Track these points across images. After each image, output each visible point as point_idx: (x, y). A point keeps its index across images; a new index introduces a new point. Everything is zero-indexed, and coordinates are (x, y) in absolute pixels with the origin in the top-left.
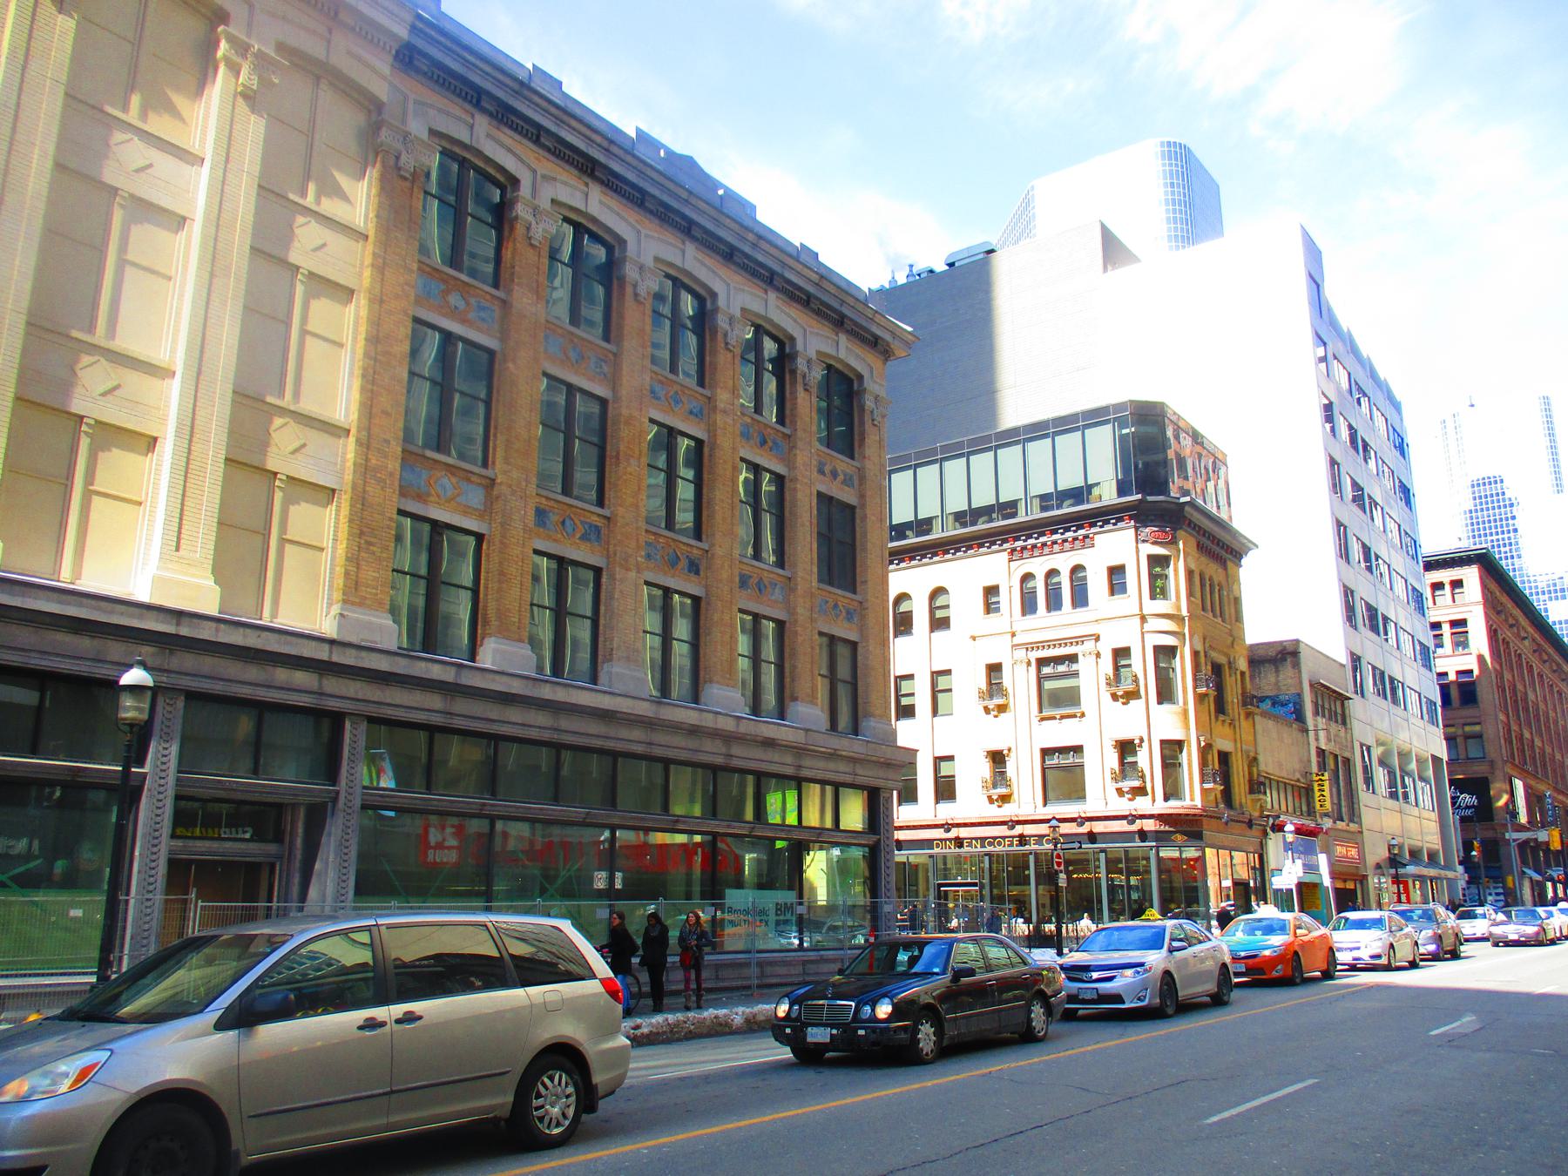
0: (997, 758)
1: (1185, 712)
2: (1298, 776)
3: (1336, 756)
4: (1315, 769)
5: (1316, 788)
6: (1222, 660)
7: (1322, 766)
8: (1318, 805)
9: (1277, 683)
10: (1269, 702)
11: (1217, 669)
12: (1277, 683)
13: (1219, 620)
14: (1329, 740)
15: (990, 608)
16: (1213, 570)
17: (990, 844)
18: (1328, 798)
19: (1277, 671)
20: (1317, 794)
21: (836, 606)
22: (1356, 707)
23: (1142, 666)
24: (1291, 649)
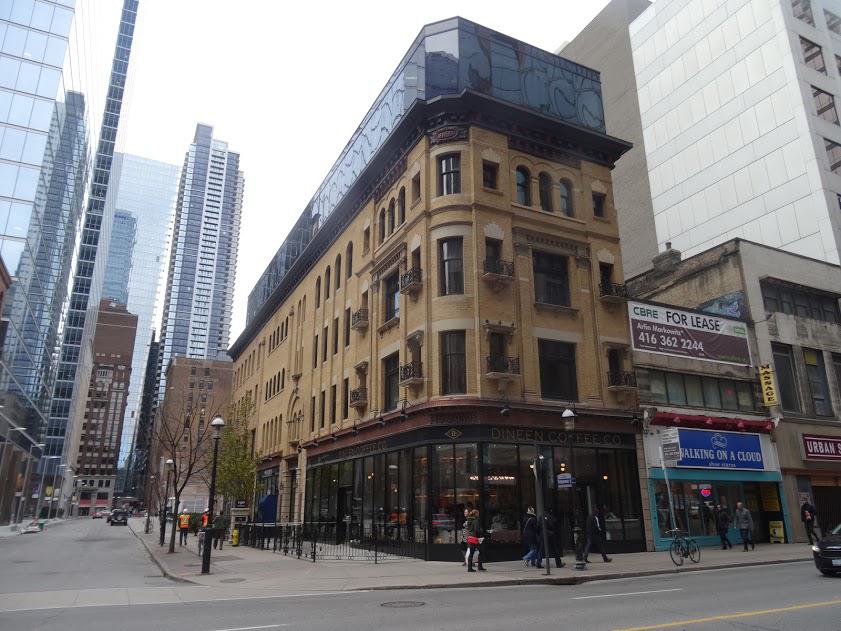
1: (469, 303)
3: (819, 353)
5: (763, 381)
8: (766, 398)
9: (722, 283)
12: (722, 283)
19: (721, 274)
20: (764, 387)
24: (730, 248)
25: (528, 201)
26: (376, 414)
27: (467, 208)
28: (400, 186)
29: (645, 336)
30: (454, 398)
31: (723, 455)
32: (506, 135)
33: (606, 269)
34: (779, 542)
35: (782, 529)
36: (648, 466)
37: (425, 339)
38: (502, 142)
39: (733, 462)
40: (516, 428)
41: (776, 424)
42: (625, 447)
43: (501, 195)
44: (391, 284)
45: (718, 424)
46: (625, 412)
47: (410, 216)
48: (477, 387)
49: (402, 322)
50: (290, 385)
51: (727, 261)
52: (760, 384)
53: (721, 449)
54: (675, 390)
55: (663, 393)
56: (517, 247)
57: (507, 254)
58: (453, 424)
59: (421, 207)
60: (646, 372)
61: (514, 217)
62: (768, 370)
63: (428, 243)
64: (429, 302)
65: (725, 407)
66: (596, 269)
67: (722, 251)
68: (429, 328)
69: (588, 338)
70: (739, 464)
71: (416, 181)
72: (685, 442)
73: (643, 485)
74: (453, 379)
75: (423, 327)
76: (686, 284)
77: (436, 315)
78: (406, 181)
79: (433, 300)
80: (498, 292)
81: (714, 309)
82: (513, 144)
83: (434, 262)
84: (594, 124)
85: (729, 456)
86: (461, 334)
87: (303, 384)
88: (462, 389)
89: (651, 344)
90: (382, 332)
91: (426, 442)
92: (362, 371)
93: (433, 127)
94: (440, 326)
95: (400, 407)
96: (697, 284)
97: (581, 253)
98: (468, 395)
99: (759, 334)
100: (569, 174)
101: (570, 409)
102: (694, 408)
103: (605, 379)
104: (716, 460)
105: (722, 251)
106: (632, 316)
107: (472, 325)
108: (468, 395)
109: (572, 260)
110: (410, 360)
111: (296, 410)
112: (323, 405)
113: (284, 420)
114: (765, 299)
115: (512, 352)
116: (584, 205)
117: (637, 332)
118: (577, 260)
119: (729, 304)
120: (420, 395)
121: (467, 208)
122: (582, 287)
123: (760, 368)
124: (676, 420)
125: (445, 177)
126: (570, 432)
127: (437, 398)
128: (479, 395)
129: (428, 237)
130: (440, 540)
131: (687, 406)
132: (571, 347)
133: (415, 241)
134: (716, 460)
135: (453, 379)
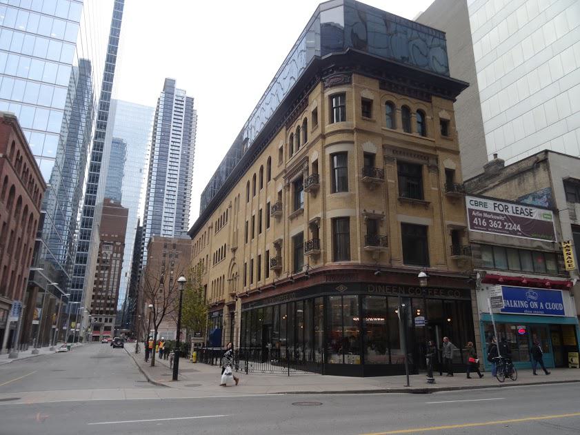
5: (565, 253)
8: (567, 265)
9: (535, 182)
10: (531, 198)
12: (535, 182)
19: (534, 176)
20: (566, 257)
24: (541, 157)
25: (393, 126)
26: (288, 274)
27: (351, 132)
28: (296, 127)
29: (478, 221)
31: (535, 305)
32: (377, 79)
33: (450, 173)
34: (576, 367)
35: (578, 358)
36: (480, 312)
37: (322, 223)
38: (375, 84)
39: (542, 310)
40: (385, 285)
41: (574, 284)
42: (462, 298)
43: (375, 122)
44: (298, 185)
45: (531, 283)
46: (463, 274)
47: (310, 139)
48: (358, 256)
49: (306, 211)
50: (229, 255)
51: (539, 167)
52: (562, 254)
53: (534, 301)
54: (499, 258)
55: (491, 261)
56: (386, 159)
57: (379, 163)
59: (318, 132)
60: (479, 246)
61: (384, 138)
62: (569, 245)
63: (323, 157)
64: (324, 198)
65: (536, 271)
66: (443, 173)
68: (324, 215)
69: (437, 223)
70: (546, 311)
71: (315, 113)
72: (507, 296)
73: (476, 325)
74: (341, 250)
75: (320, 215)
76: (508, 183)
77: (332, 206)
78: (308, 114)
79: (327, 196)
80: (372, 190)
81: (529, 201)
82: (383, 86)
83: (328, 170)
84: (441, 70)
85: (539, 305)
86: (346, 220)
87: (238, 254)
88: (347, 257)
89: (482, 226)
90: (292, 218)
91: (322, 294)
92: (278, 245)
93: (326, 75)
94: (332, 214)
95: (304, 269)
96: (517, 183)
97: (432, 162)
98: (352, 262)
99: (562, 219)
100: (423, 106)
101: (424, 272)
102: (513, 271)
103: (449, 251)
104: (529, 309)
105: (535, 159)
106: (469, 206)
108: (352, 262)
109: (425, 167)
110: (311, 238)
111: (234, 272)
112: (252, 269)
113: (226, 278)
114: (567, 193)
115: (382, 232)
116: (434, 129)
117: (472, 218)
118: (428, 166)
119: (540, 198)
120: (318, 261)
121: (351, 132)
122: (433, 186)
123: (563, 243)
124: (501, 280)
125: (335, 110)
126: (424, 288)
127: (330, 264)
128: (359, 262)
129: (323, 152)
130: (332, 361)
131: (508, 270)
132: (424, 229)
133: (314, 155)
134: (529, 309)
135: (341, 250)
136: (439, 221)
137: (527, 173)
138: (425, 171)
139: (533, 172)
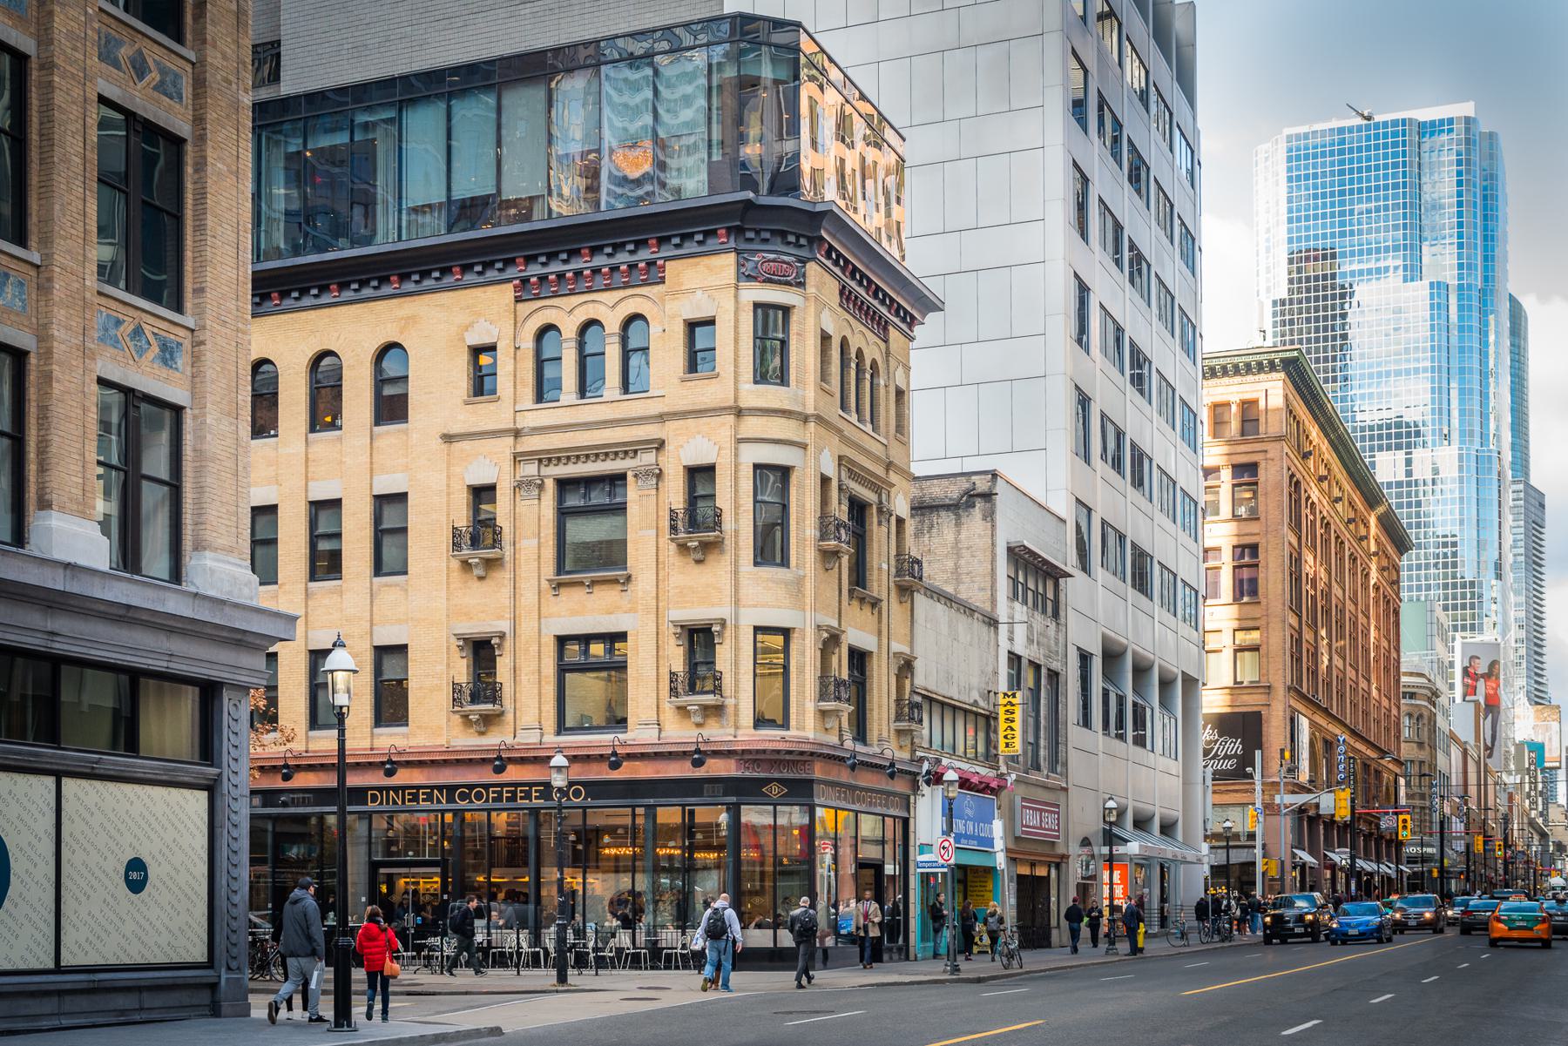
0: (482, 651)
2: (975, 696)
3: (1037, 667)
4: (1003, 686)
5: (1002, 717)
6: (868, 495)
7: (1015, 682)
8: (1002, 742)
9: (957, 542)
11: (858, 509)
12: (957, 542)
13: (868, 428)
14: (1030, 641)
15: (481, 384)
16: (863, 339)
17: (463, 797)
18: (1018, 733)
20: (1002, 725)
21: (138, 332)
22: (1075, 589)
23: (735, 502)
24: (982, 485)
30: (769, 738)
52: (996, 719)
58: (776, 775)
62: (1014, 701)
67: (966, 486)
91: (734, 799)
94: (751, 617)
105: (964, 484)
107: (807, 623)
118: (880, 511)
128: (810, 734)
136: (885, 641)
137: (943, 513)
138: (873, 517)
139: (958, 517)
